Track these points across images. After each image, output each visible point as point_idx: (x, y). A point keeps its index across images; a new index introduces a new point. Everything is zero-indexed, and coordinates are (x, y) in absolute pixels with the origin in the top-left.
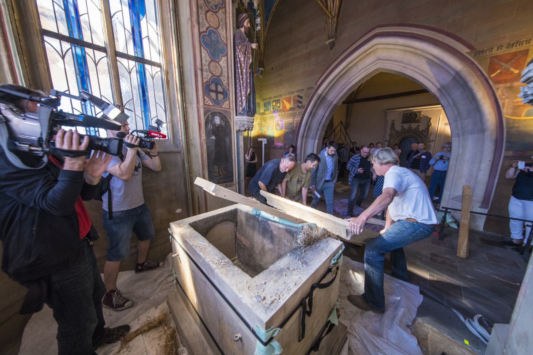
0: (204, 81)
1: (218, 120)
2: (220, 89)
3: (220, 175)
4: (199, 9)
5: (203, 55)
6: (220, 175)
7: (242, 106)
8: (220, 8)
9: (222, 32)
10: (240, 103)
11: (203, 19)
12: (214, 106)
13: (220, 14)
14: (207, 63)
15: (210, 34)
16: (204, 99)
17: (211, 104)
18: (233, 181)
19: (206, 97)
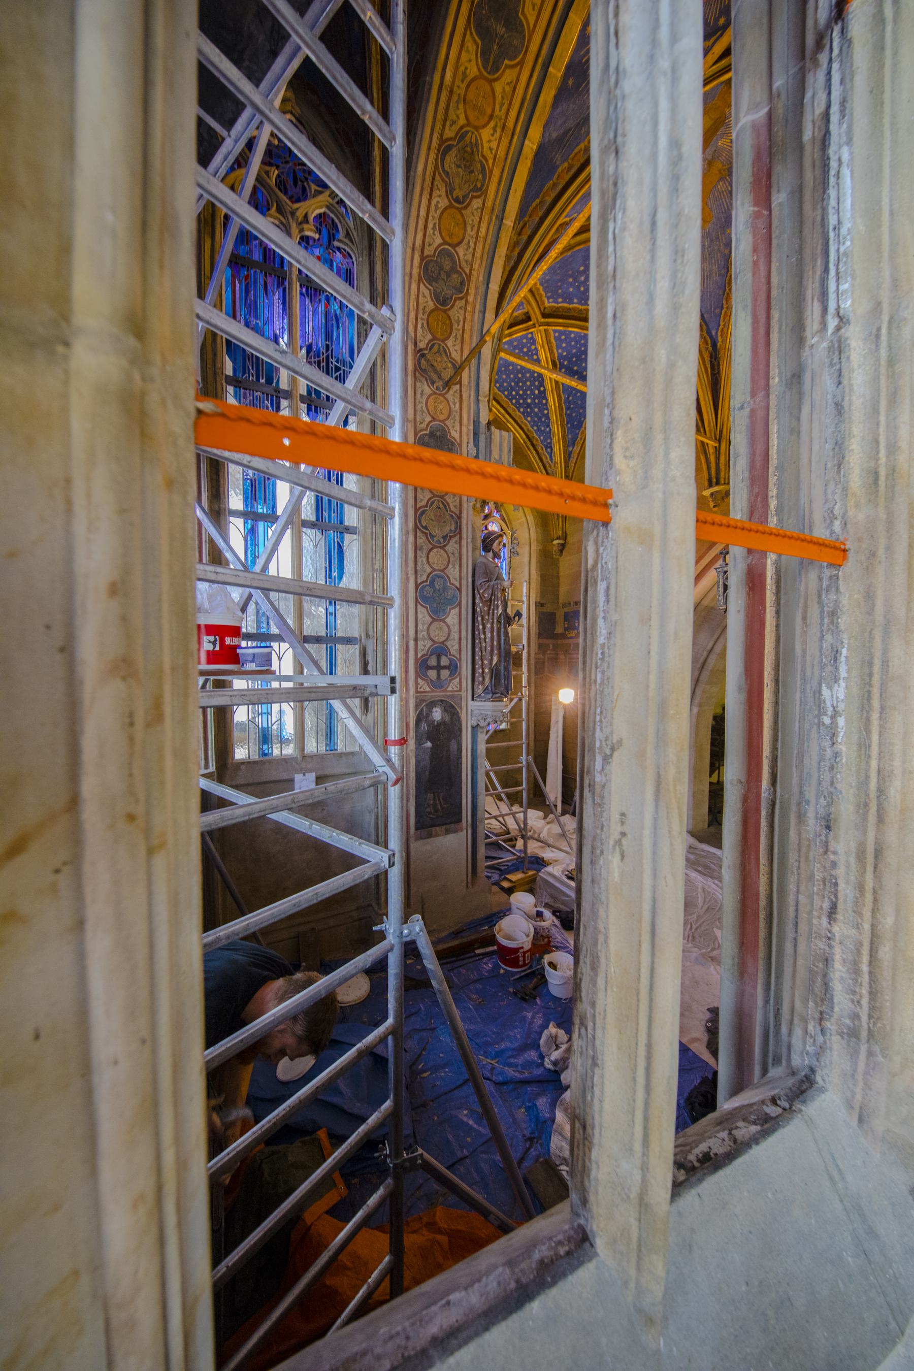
0: (419, 656)
1: (437, 714)
2: (444, 661)
3: (436, 811)
4: (418, 552)
5: (420, 616)
6: (436, 811)
7: (483, 683)
8: (451, 537)
9: (453, 572)
10: (481, 679)
11: (423, 564)
12: (433, 691)
13: (452, 546)
14: (425, 627)
15: (433, 581)
16: (417, 683)
17: (428, 689)
18: (460, 820)
19: (420, 680)
